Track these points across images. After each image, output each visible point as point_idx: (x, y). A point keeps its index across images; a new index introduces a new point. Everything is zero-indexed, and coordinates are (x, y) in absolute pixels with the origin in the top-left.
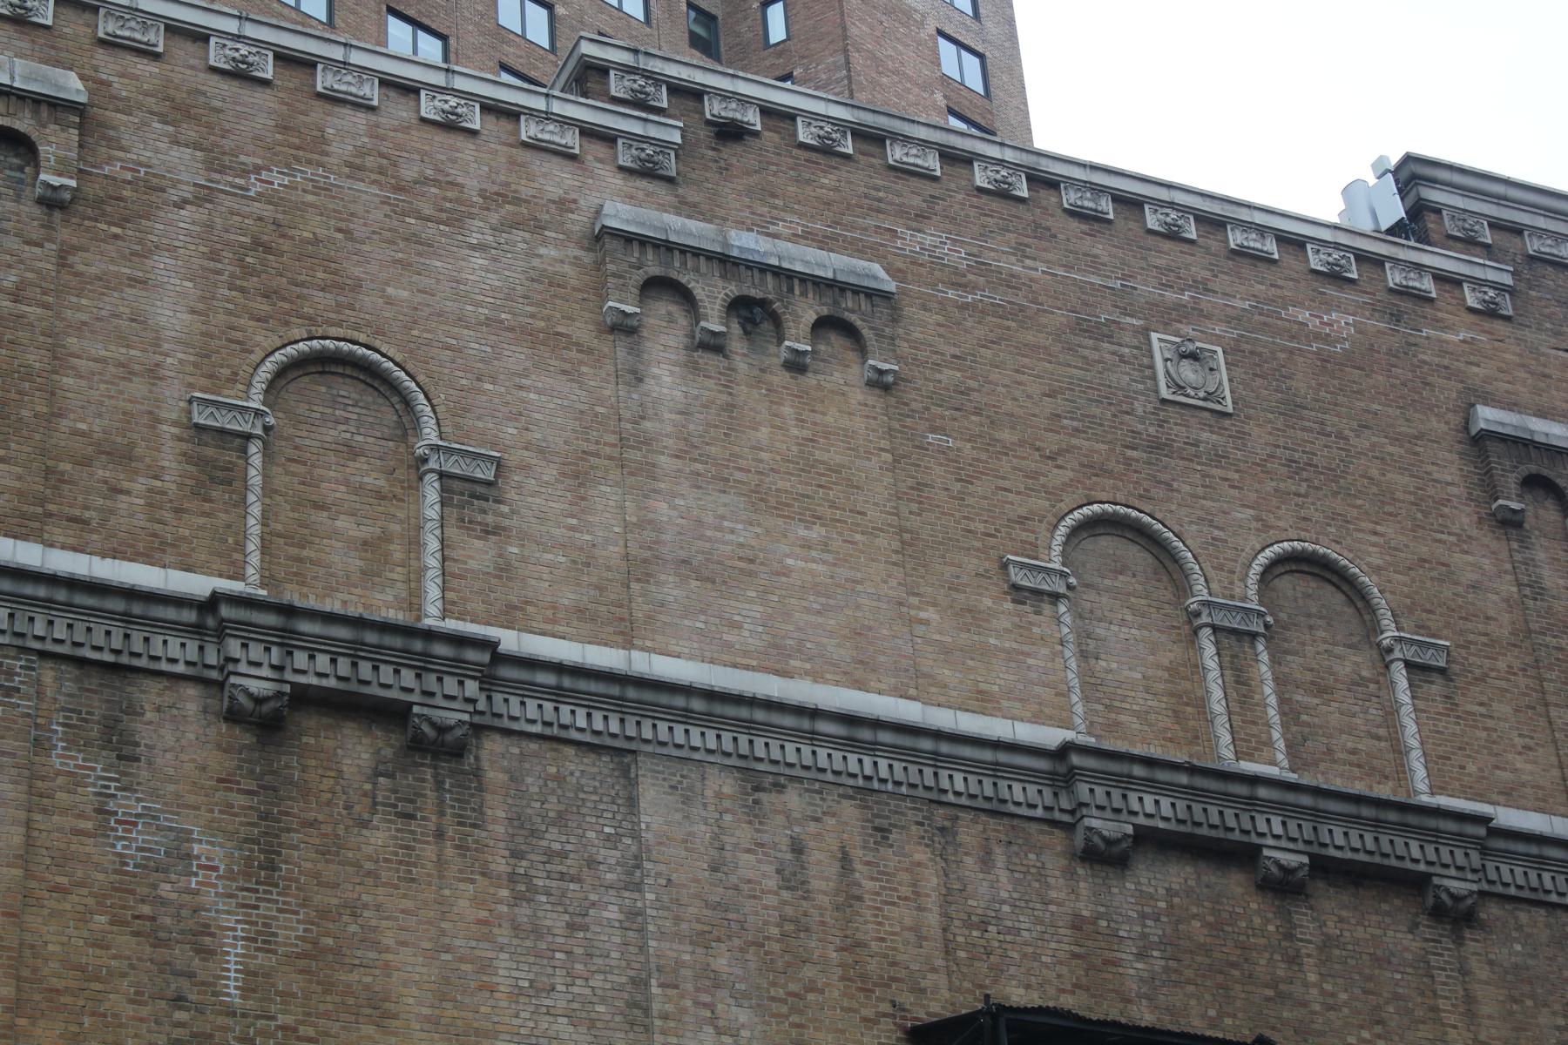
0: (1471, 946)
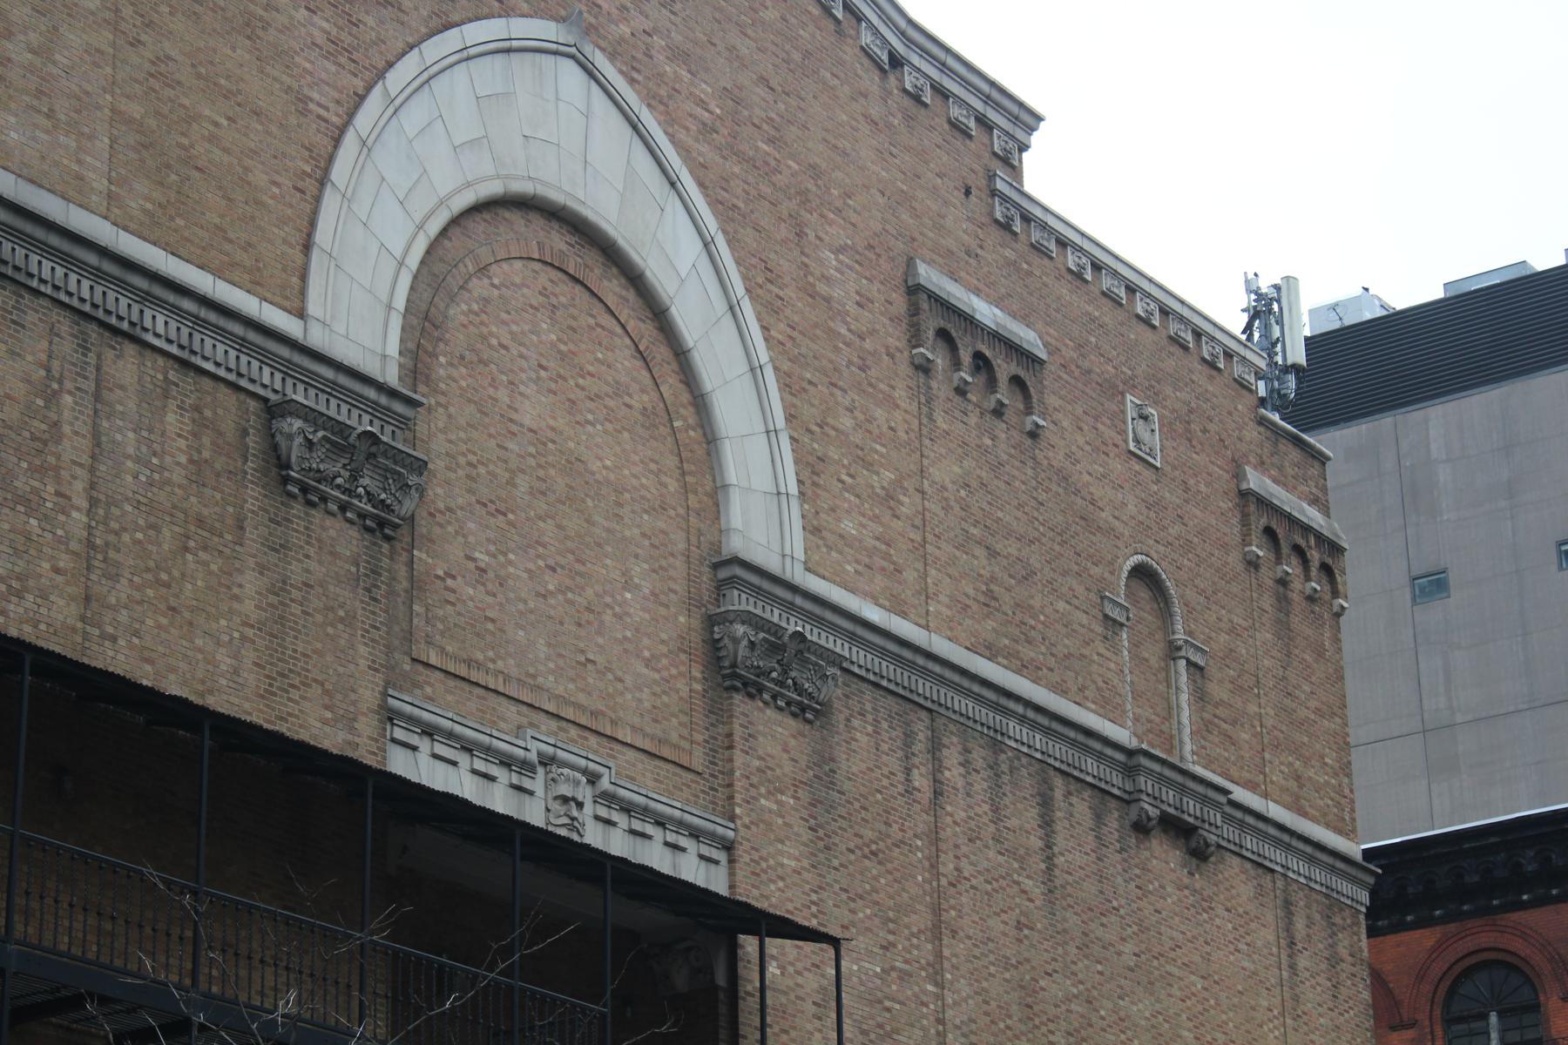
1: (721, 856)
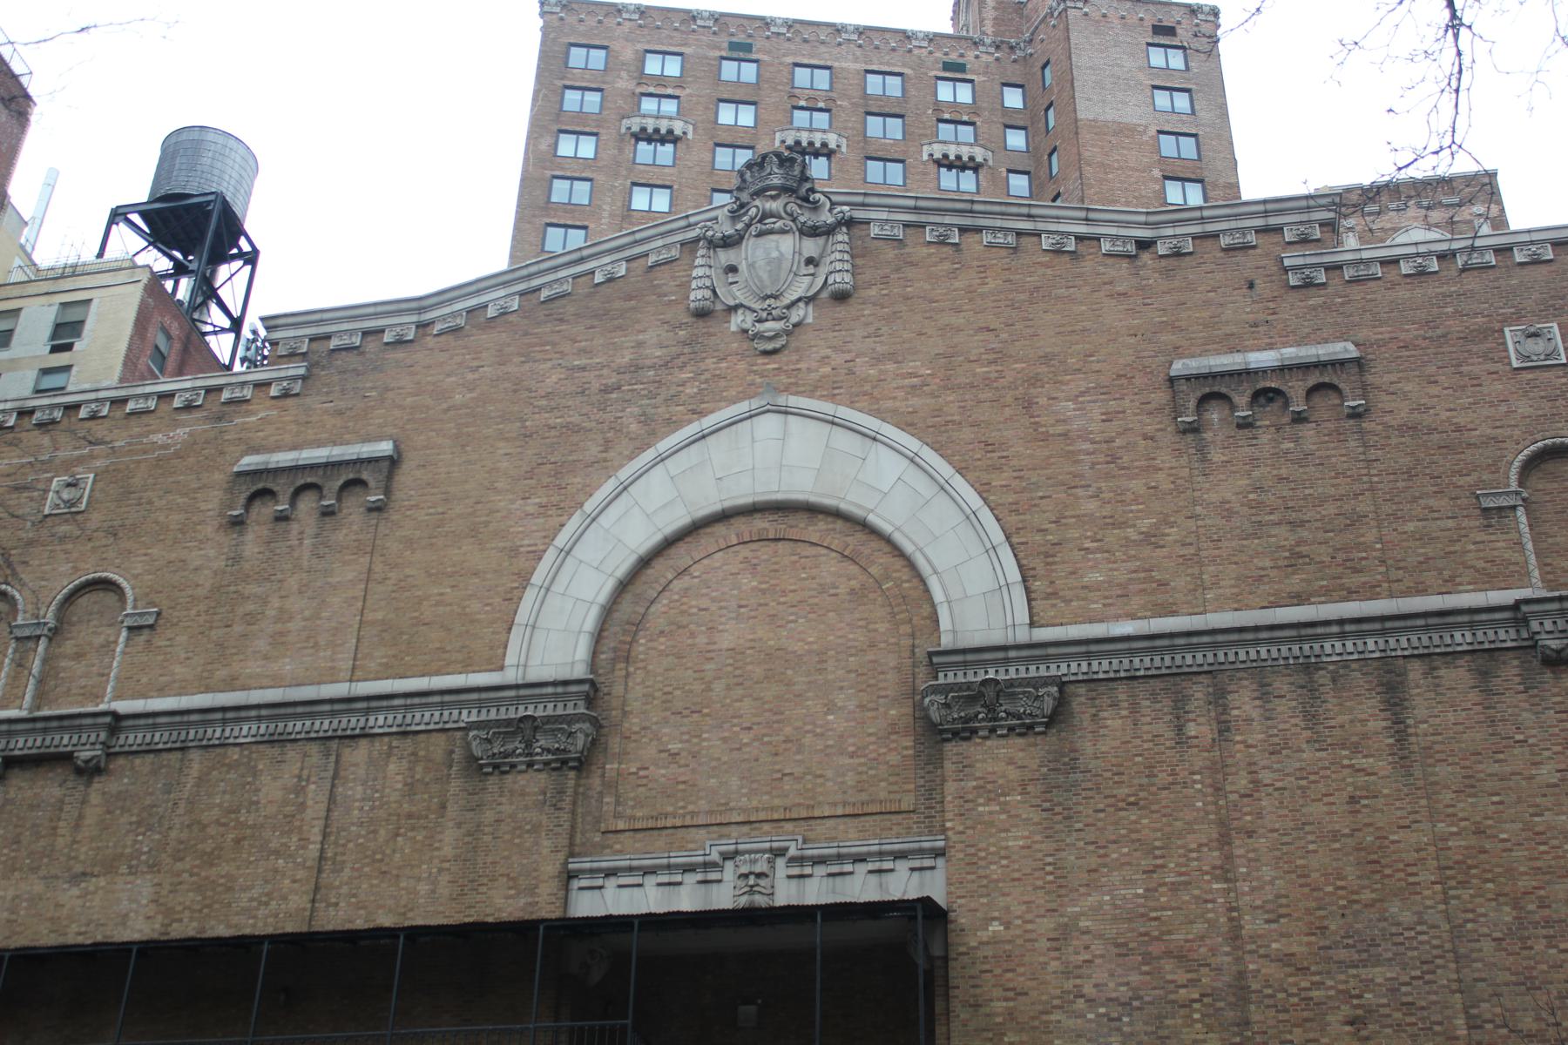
0: (96, 786)
1: (940, 862)
